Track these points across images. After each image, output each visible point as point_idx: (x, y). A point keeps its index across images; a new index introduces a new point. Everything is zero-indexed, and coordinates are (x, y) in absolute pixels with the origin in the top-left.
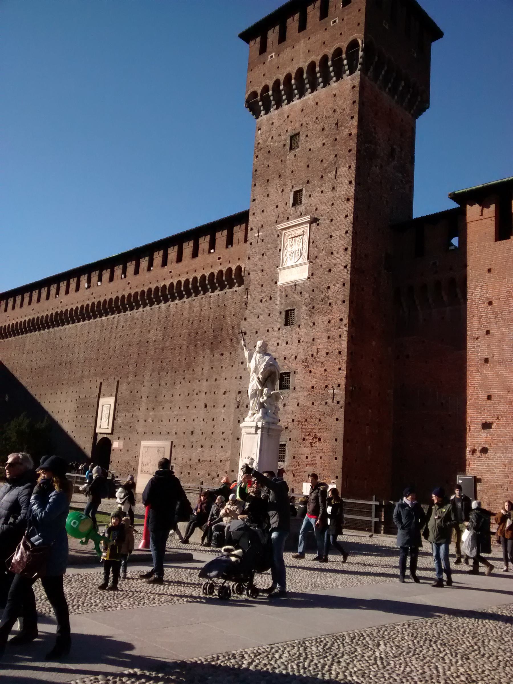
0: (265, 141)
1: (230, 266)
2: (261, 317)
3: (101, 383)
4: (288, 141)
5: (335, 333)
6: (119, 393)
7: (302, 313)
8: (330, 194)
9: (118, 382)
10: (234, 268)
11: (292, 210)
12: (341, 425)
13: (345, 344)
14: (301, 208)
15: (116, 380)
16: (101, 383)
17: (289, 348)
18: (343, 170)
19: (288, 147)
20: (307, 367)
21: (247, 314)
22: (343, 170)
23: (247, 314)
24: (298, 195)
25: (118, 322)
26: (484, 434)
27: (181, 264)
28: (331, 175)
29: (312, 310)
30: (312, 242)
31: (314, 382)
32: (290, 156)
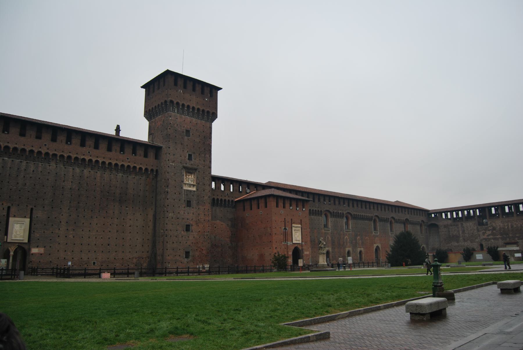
0: (174, 125)
1: (135, 165)
2: (176, 200)
3: (9, 208)
4: (185, 131)
6: (34, 216)
7: (194, 203)
9: (32, 209)
10: (138, 167)
11: (188, 161)
14: (192, 162)
15: (30, 207)
16: (9, 208)
19: (185, 134)
20: (197, 224)
23: (168, 197)
24: (190, 156)
27: (97, 151)
28: (203, 155)
31: (200, 230)
32: (186, 138)
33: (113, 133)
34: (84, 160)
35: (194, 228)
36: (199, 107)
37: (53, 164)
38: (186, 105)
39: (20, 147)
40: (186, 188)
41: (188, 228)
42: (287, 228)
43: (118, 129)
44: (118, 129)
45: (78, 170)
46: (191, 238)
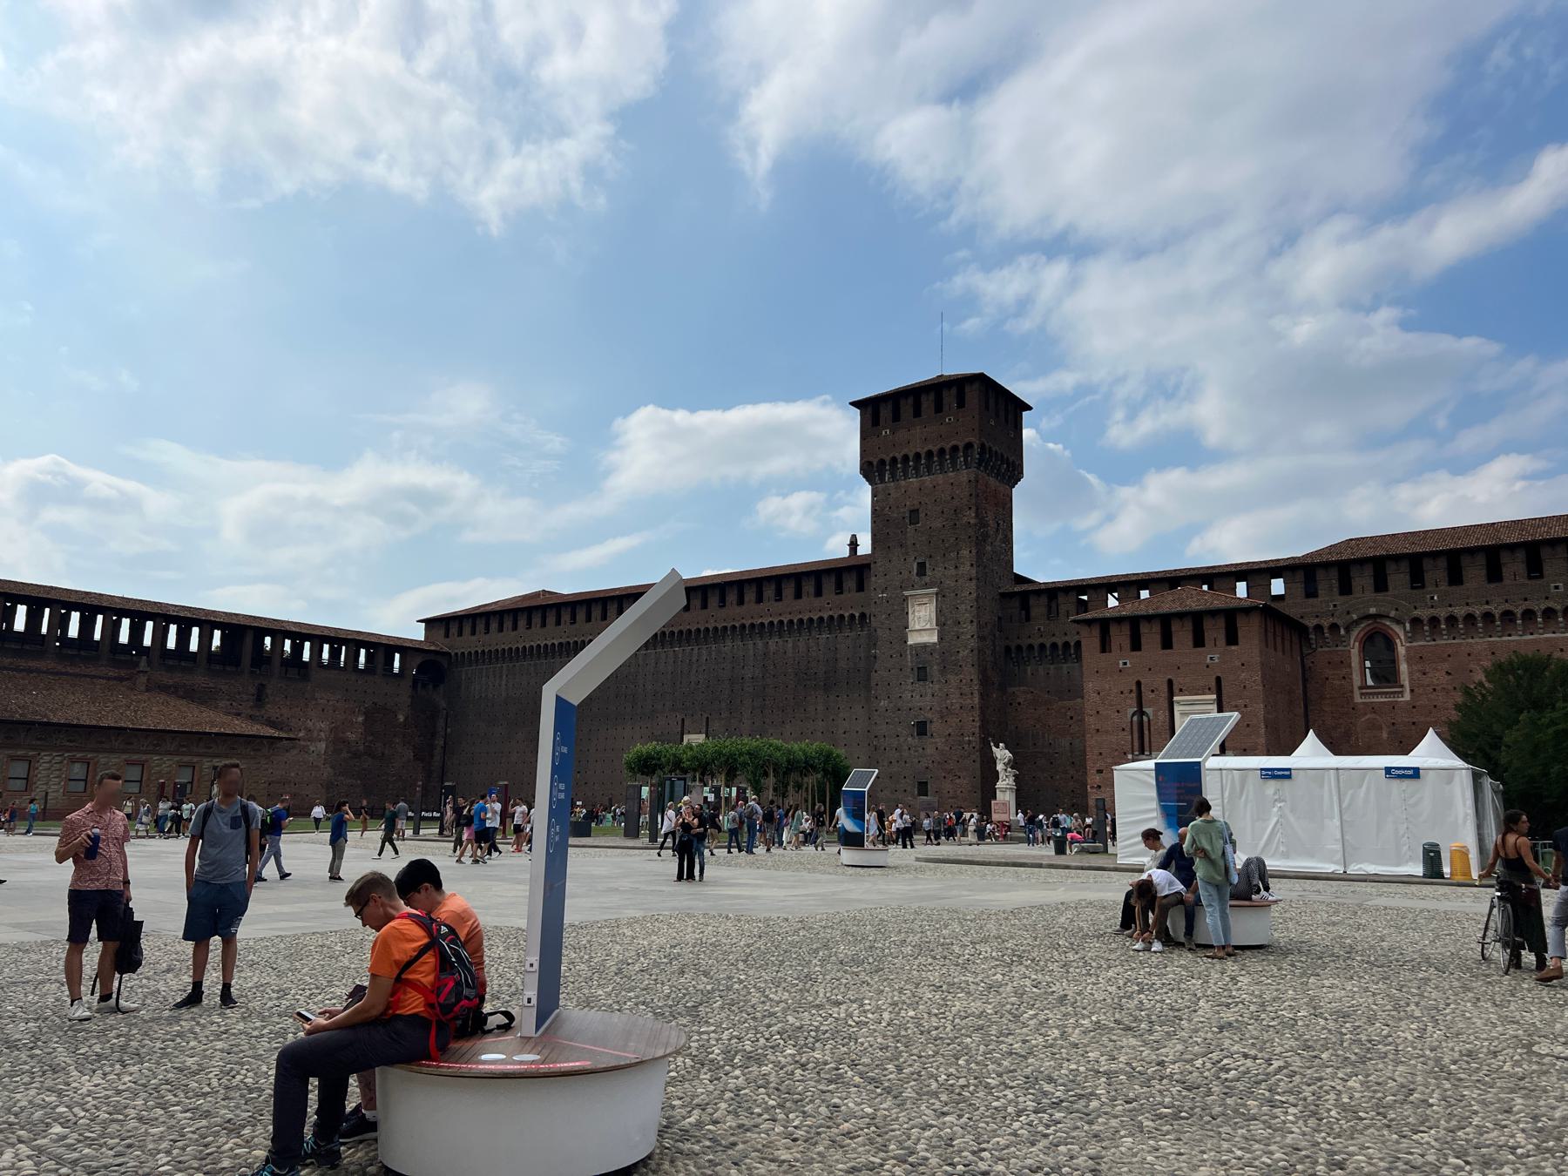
5: (966, 690)
7: (934, 670)
8: (953, 572)
12: (978, 765)
13: (977, 700)
14: (927, 579)
17: (921, 699)
18: (965, 553)
21: (877, 667)
22: (965, 553)
24: (922, 566)
25: (699, 655)
26: (1098, 777)
29: (944, 670)
30: (939, 612)
33: (846, 553)
34: (762, 624)
35: (936, 727)
36: (930, 447)
37: (729, 643)
38: (899, 456)
39: (685, 628)
40: (912, 640)
41: (922, 729)
42: (1148, 710)
43: (854, 544)
44: (854, 544)
45: (760, 644)
46: (930, 750)
